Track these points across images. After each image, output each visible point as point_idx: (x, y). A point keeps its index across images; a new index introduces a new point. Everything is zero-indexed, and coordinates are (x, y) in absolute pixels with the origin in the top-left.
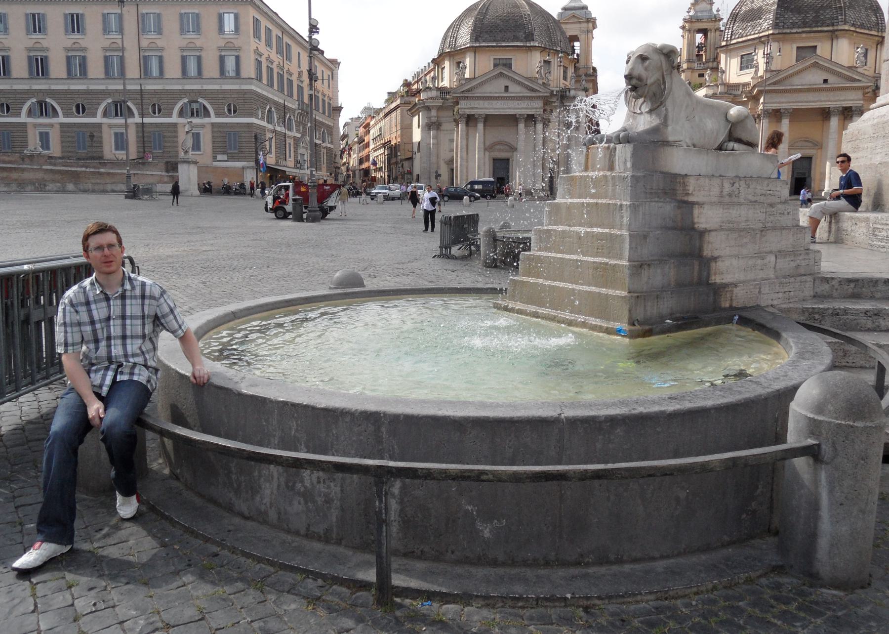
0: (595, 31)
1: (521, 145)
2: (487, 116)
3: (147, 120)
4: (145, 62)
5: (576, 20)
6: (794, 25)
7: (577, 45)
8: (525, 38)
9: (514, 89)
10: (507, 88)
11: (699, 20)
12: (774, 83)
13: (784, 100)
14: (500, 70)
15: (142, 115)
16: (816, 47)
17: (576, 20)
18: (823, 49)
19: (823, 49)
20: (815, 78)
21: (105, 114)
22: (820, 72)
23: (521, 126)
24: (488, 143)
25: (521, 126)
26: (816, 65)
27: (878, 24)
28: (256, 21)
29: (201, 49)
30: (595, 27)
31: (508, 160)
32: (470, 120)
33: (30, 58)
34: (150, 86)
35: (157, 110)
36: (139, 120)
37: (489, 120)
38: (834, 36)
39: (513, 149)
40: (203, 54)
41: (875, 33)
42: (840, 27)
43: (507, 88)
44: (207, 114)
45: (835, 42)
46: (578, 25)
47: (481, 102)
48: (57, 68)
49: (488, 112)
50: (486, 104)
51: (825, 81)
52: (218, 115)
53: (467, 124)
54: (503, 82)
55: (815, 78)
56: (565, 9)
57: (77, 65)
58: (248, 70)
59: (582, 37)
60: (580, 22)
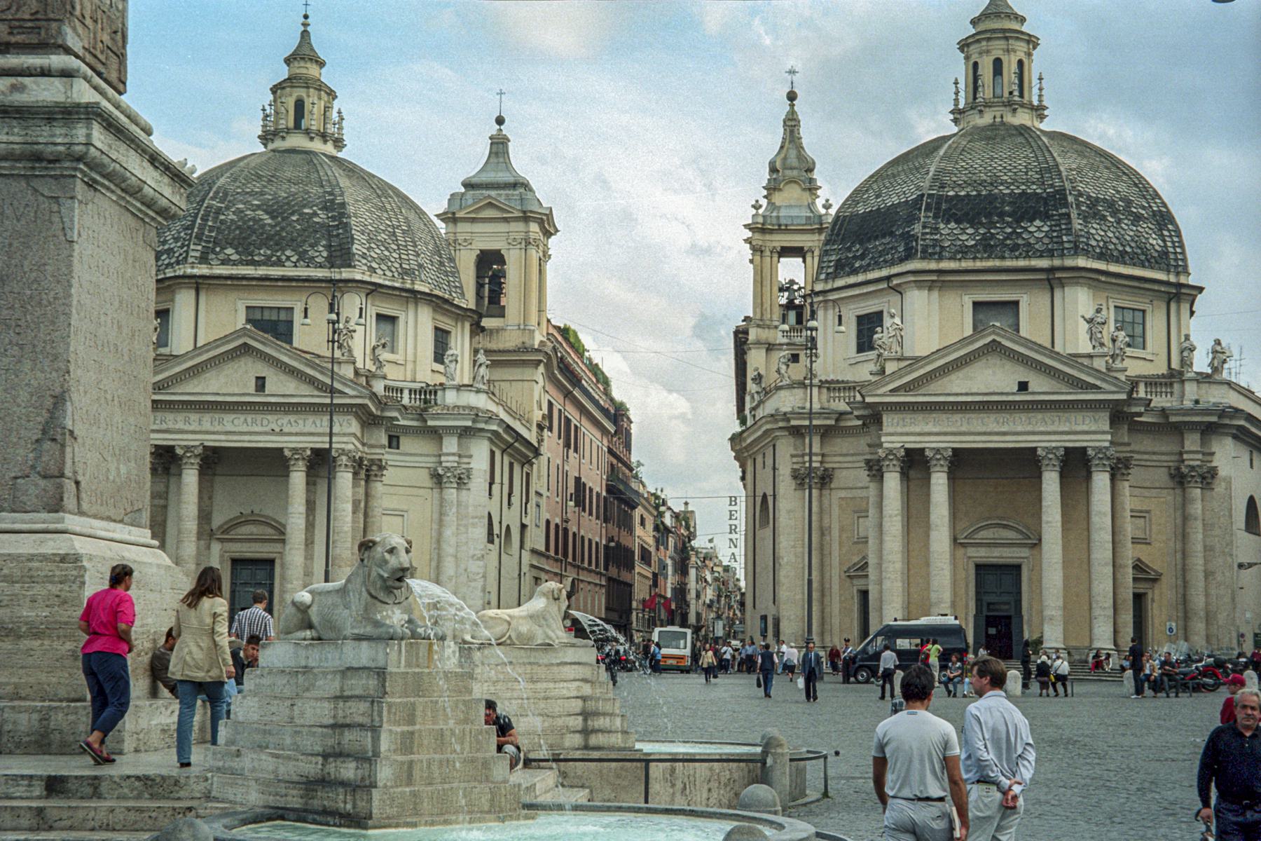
1: (296, 521)
2: (216, 451)
5: (498, 214)
6: (964, 252)
8: (329, 259)
9: (281, 387)
10: (261, 383)
11: (782, 229)
12: (906, 388)
13: (928, 428)
16: (1016, 303)
17: (498, 214)
18: (1032, 307)
19: (1032, 307)
20: (994, 379)
22: (1009, 365)
24: (218, 520)
26: (994, 348)
27: (1167, 253)
31: (271, 562)
37: (215, 461)
38: (1053, 280)
39: (280, 534)
41: (1161, 276)
42: (1069, 262)
43: (261, 383)
45: (1058, 294)
46: (502, 227)
47: (194, 417)
50: (207, 421)
51: (1023, 386)
54: (257, 368)
55: (994, 379)
56: (468, 185)
59: (513, 259)
60: (506, 220)
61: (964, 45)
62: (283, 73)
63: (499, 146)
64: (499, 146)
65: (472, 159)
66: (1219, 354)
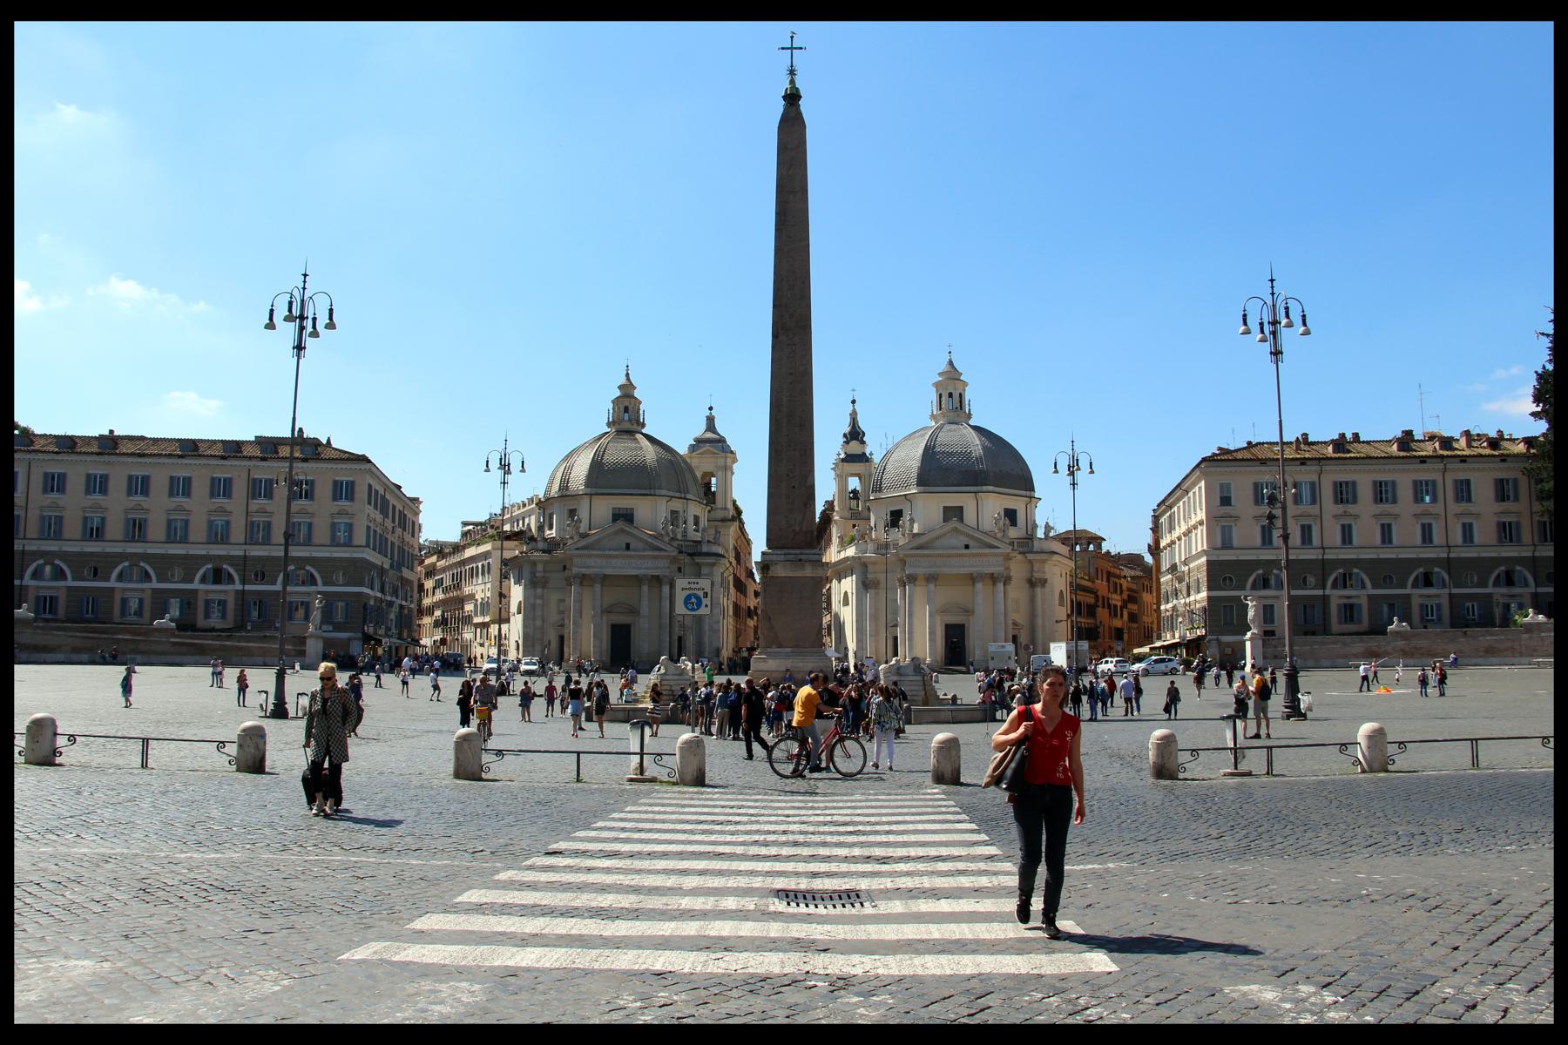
0: (735, 466)
3: (247, 587)
4: (251, 527)
7: (714, 480)
14: (620, 524)
15: (243, 582)
21: (203, 580)
23: (645, 588)
25: (645, 588)
28: (370, 486)
29: (313, 514)
30: (735, 460)
32: (584, 580)
33: (127, 521)
34: (257, 551)
35: (262, 577)
36: (240, 587)
39: (635, 612)
40: (315, 521)
44: (313, 582)
48: (156, 530)
49: (609, 571)
52: (325, 584)
53: (581, 584)
57: (177, 531)
58: (360, 537)
61: (937, 385)
62: (618, 393)
63: (710, 421)
64: (710, 421)
65: (699, 429)
66: (1048, 528)
